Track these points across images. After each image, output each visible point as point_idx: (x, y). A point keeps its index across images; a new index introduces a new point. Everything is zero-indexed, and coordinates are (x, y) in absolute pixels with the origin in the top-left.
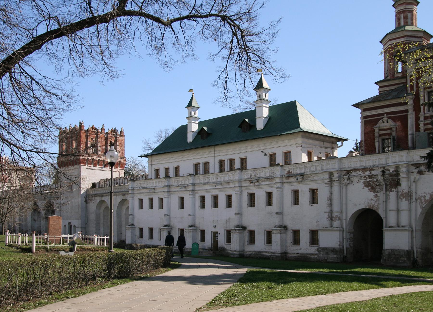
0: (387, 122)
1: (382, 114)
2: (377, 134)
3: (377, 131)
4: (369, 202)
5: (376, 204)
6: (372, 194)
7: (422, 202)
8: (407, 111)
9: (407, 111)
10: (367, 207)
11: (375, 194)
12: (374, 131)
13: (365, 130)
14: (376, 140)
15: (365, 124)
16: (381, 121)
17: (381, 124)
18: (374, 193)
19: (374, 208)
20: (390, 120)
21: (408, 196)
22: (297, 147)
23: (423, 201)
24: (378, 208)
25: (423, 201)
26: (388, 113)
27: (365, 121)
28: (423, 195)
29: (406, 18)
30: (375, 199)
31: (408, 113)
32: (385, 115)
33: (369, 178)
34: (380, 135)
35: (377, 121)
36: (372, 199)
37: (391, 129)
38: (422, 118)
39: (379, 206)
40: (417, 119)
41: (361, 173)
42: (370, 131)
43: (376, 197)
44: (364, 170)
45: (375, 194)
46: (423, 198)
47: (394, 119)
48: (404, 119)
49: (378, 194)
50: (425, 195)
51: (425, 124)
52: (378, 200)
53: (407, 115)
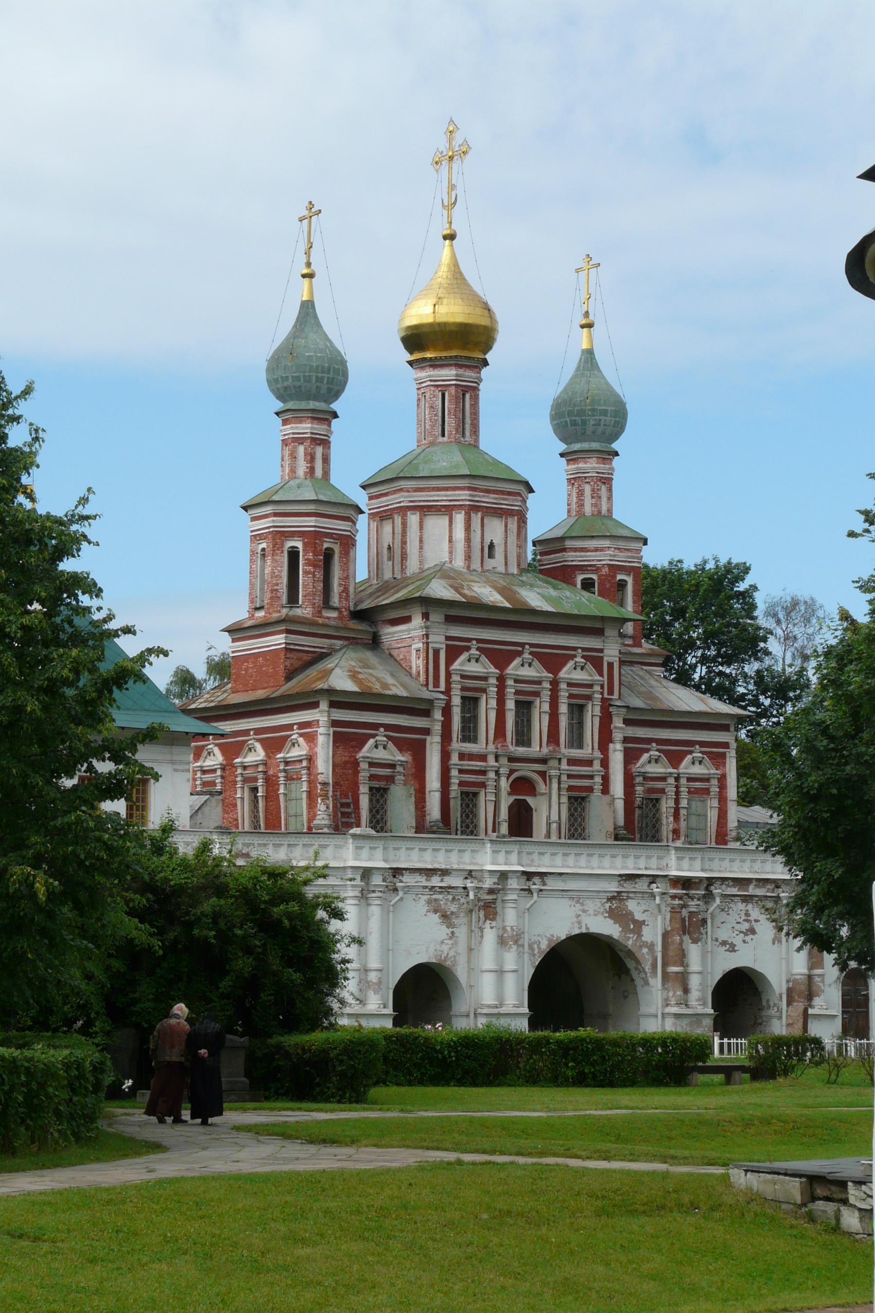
0: (385, 747)
1: (376, 726)
2: (363, 775)
3: (364, 766)
4: (438, 947)
5: (452, 953)
6: (443, 931)
7: (534, 955)
8: (427, 731)
9: (427, 731)
10: (434, 961)
11: (449, 931)
12: (356, 763)
13: (333, 756)
14: (364, 789)
15: (334, 742)
16: (371, 741)
17: (367, 750)
18: (448, 927)
19: (448, 963)
20: (390, 745)
21: (517, 939)
22: (176, 770)
23: (536, 952)
24: (455, 963)
25: (536, 952)
26: (388, 727)
27: (334, 732)
28: (536, 938)
29: (311, 458)
30: (450, 942)
31: (428, 738)
32: (382, 730)
33: (440, 893)
34: (372, 777)
35: (362, 741)
36: (442, 942)
37: (392, 766)
38: (455, 759)
39: (457, 958)
40: (445, 756)
41: (422, 880)
42: (346, 762)
43: (450, 938)
44: (429, 872)
45: (449, 931)
46: (535, 946)
47: (401, 745)
48: (418, 750)
49: (454, 930)
50: (540, 939)
51: (461, 771)
52: (456, 943)
53: (425, 740)
